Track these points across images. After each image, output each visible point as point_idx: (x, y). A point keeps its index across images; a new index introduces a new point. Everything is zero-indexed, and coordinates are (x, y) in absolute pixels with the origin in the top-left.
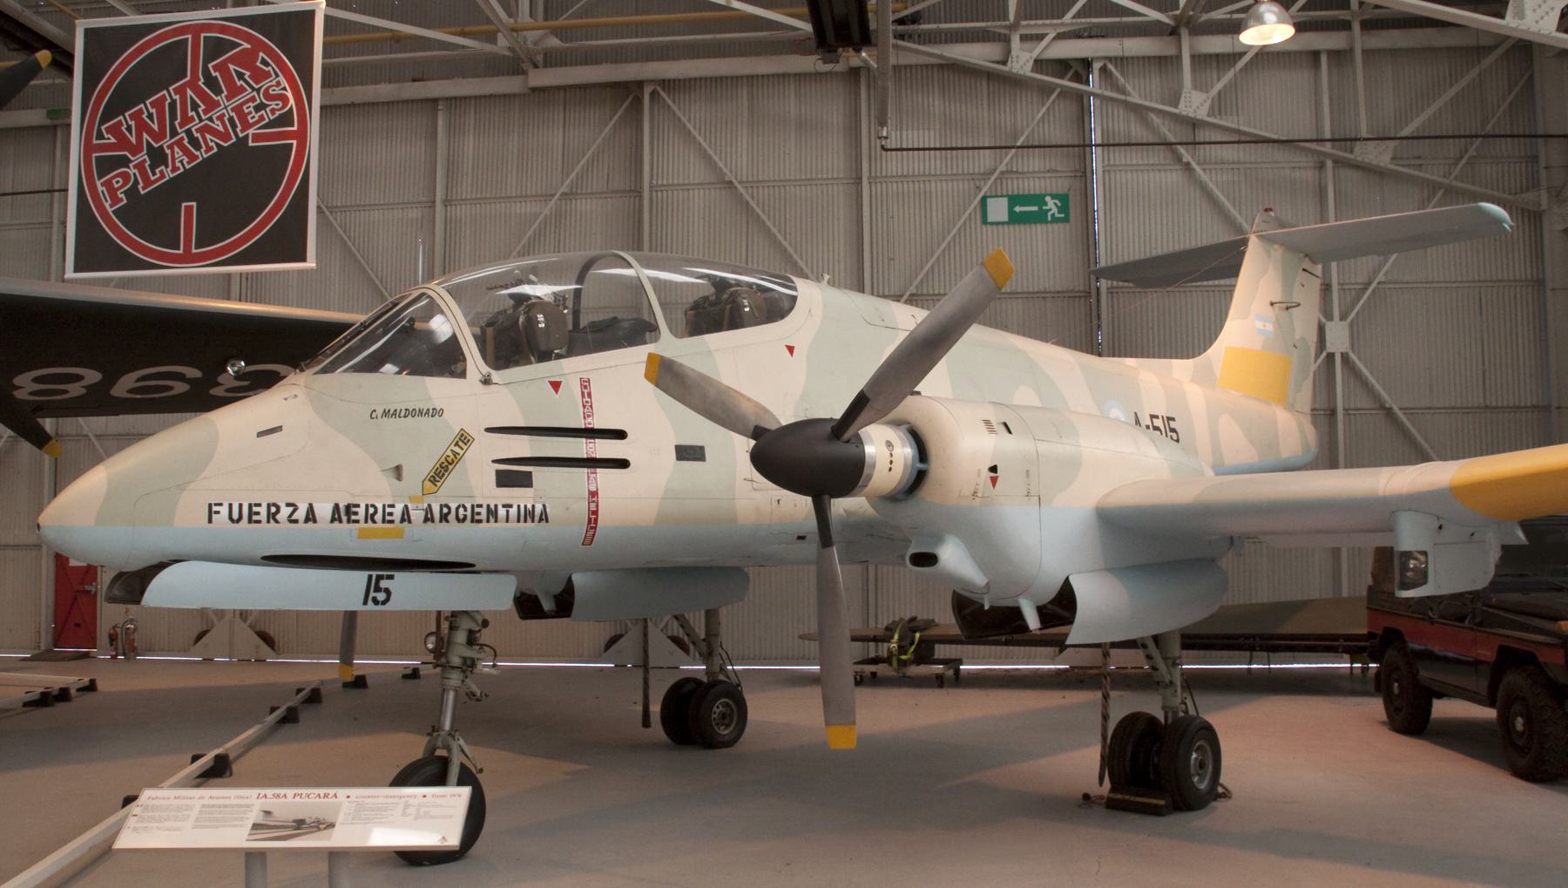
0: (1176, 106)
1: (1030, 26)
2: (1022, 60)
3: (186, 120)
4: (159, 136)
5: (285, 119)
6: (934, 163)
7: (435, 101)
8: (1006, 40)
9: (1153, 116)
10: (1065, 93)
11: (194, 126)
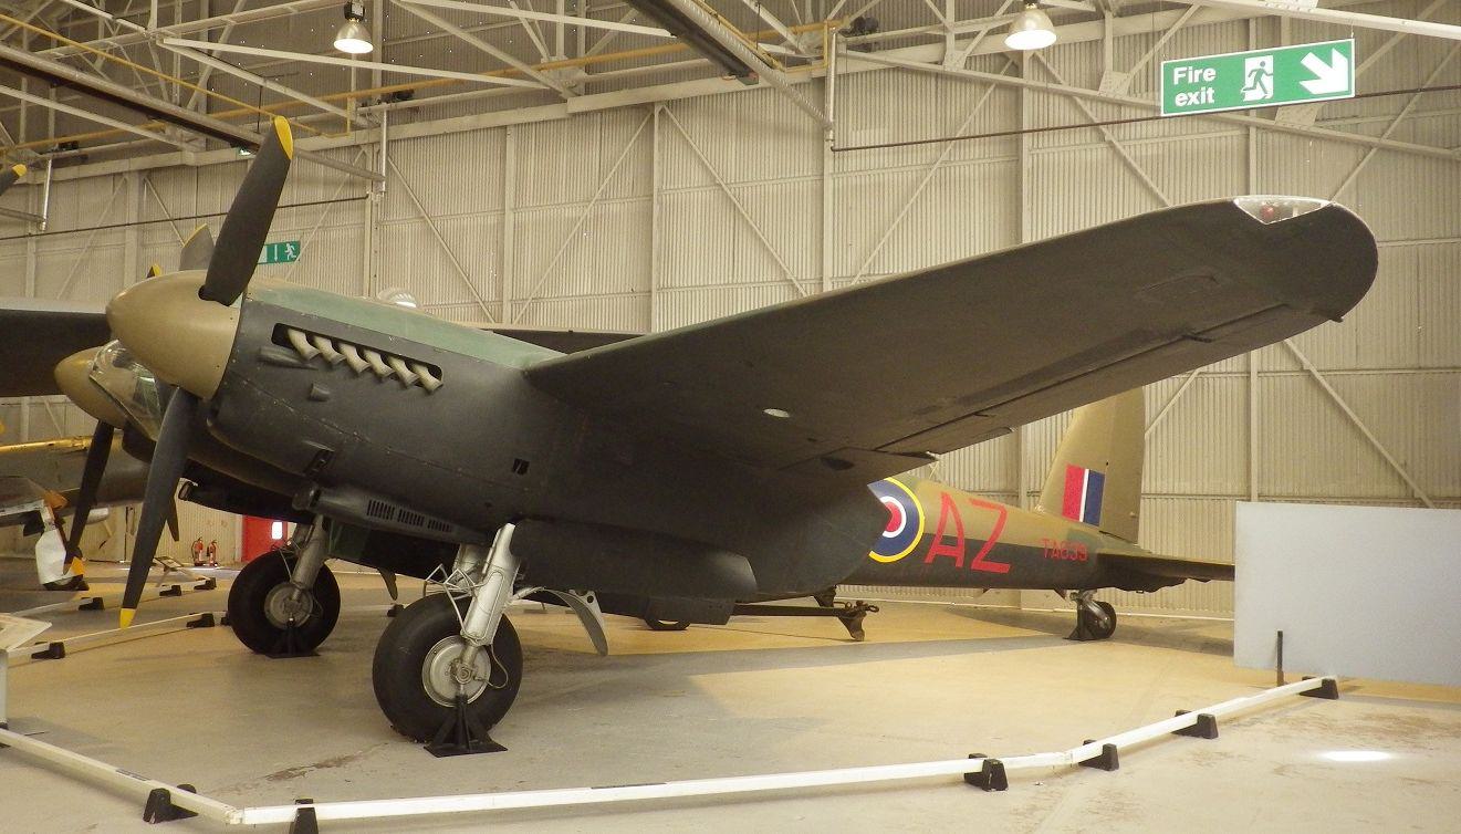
0: (1097, 88)
1: (968, 27)
2: (955, 61)
6: (887, 157)
7: (505, 127)
8: (941, 40)
9: (1078, 100)
10: (1001, 86)
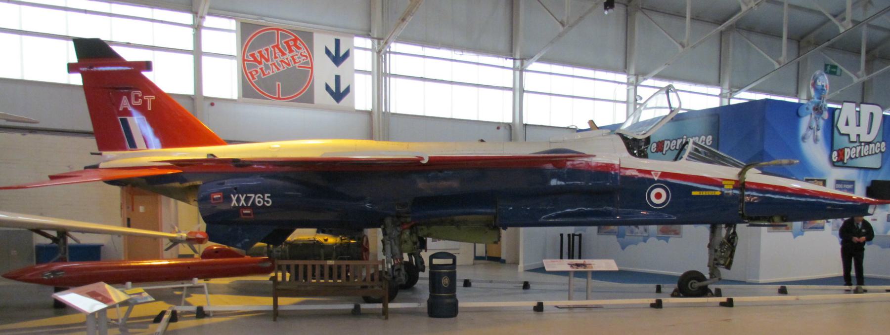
3: (276, 57)
4: (267, 60)
5: (307, 63)
11: (278, 60)
